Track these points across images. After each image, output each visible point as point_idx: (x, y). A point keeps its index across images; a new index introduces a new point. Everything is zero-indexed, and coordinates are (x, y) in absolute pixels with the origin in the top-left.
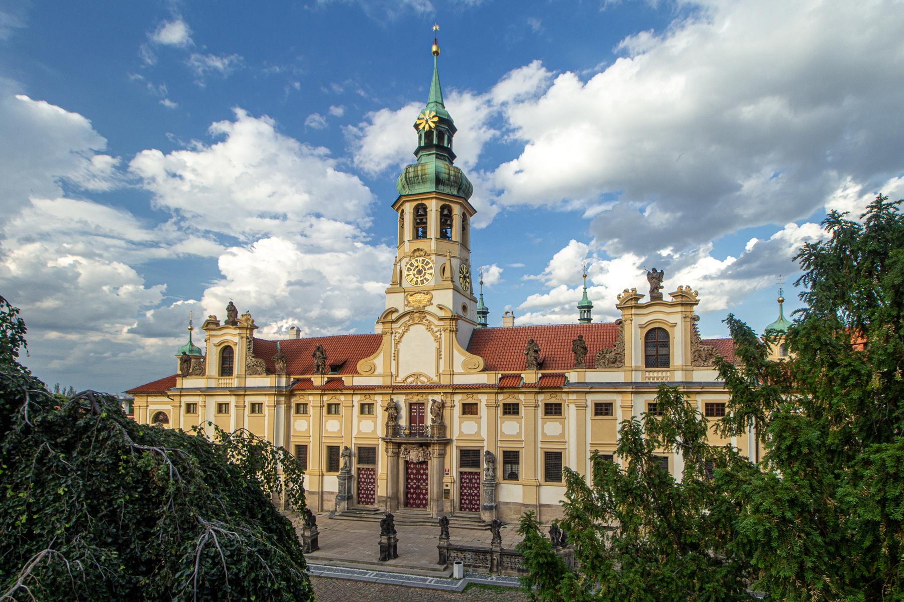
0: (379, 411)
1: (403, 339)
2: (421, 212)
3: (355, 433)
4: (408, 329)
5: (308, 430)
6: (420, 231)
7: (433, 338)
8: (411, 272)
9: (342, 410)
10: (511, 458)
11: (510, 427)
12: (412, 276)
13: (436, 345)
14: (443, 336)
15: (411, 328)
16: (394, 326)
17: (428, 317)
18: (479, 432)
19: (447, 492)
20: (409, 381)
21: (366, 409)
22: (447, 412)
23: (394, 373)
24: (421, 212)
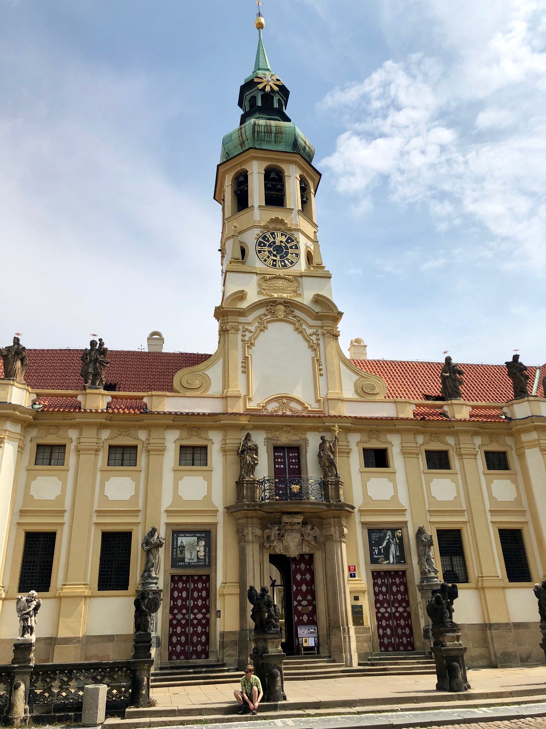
0: (216, 457)
1: (257, 342)
2: (273, 175)
3: (166, 502)
4: (265, 328)
5: (61, 499)
6: (275, 196)
7: (306, 344)
8: (266, 248)
9: (142, 459)
10: (451, 542)
11: (443, 488)
12: (267, 253)
13: (310, 354)
14: (321, 342)
15: (270, 326)
16: (242, 319)
17: (297, 313)
18: (395, 497)
19: (357, 612)
20: (272, 407)
21: (193, 455)
22: (339, 461)
23: (243, 393)
24: (273, 175)
